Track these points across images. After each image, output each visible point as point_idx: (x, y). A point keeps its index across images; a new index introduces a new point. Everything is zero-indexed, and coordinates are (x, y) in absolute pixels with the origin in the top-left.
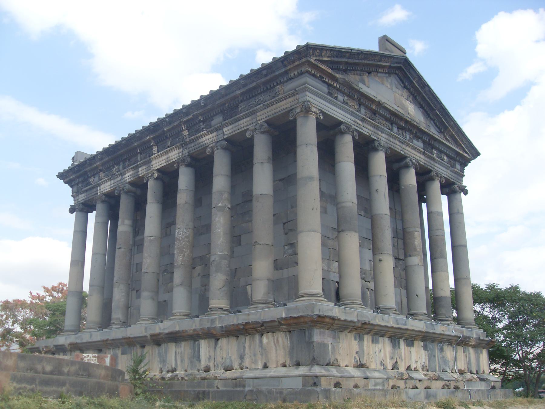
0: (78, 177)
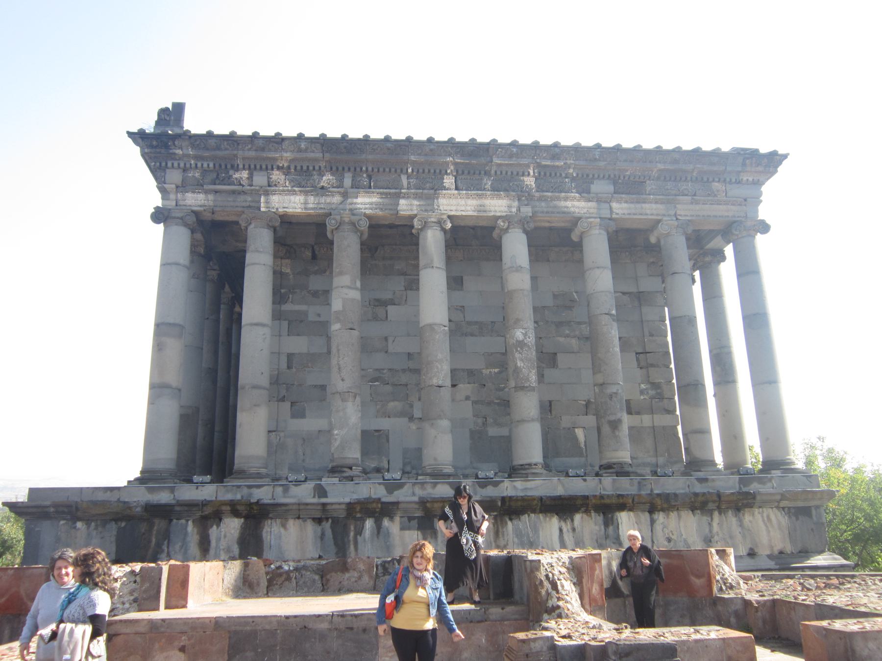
0: (197, 158)
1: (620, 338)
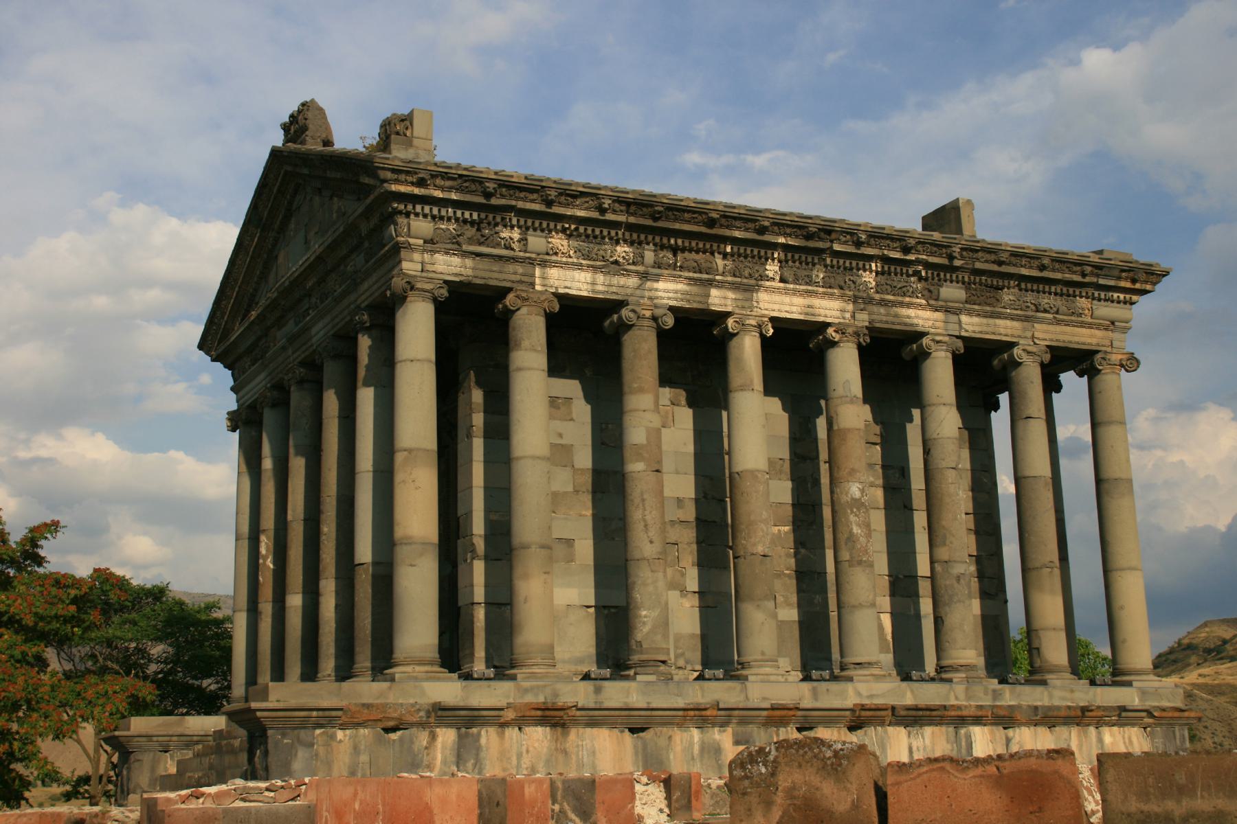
0: (457, 204)
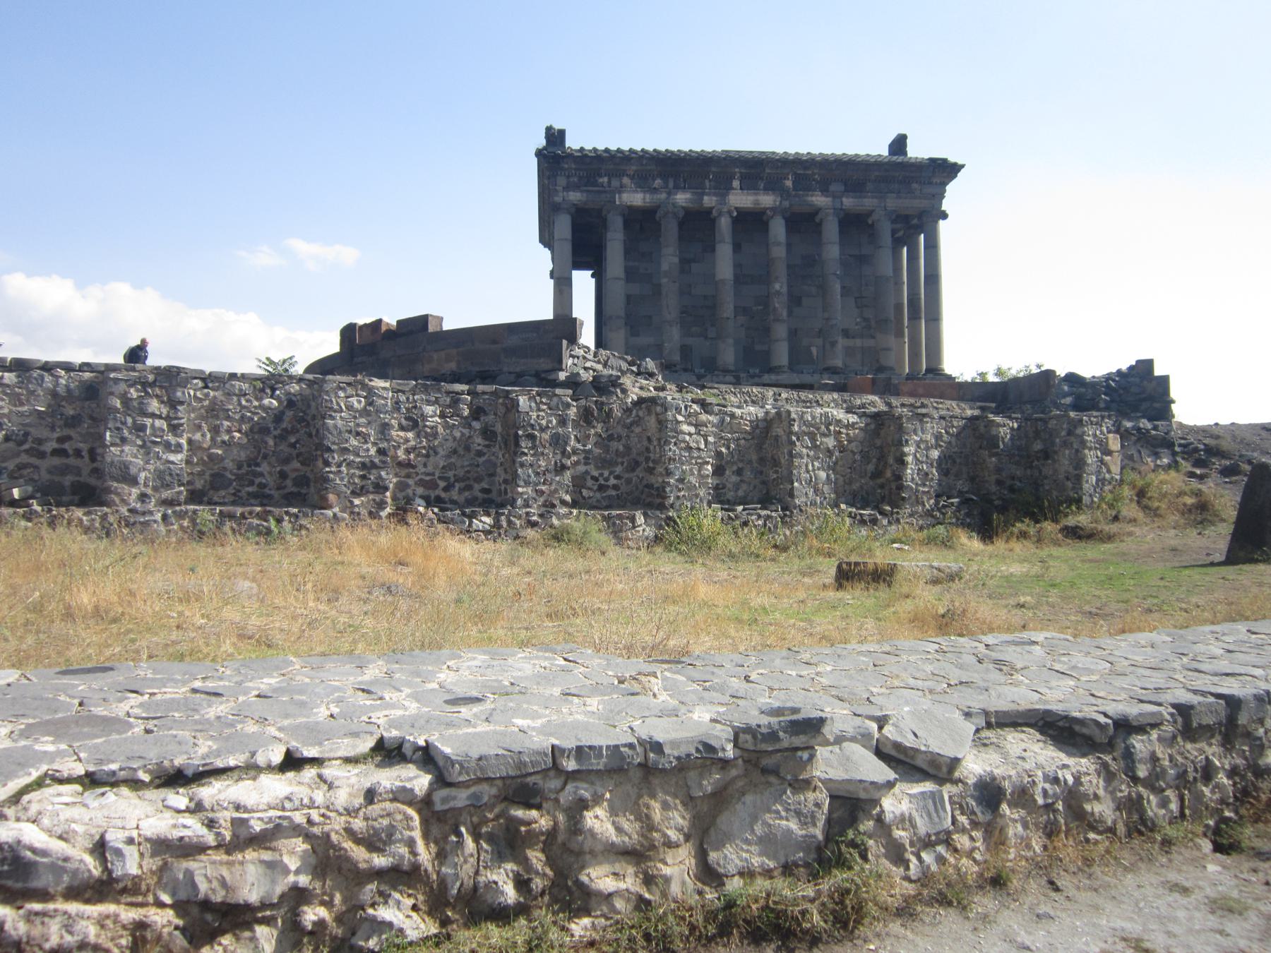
1: (843, 288)
